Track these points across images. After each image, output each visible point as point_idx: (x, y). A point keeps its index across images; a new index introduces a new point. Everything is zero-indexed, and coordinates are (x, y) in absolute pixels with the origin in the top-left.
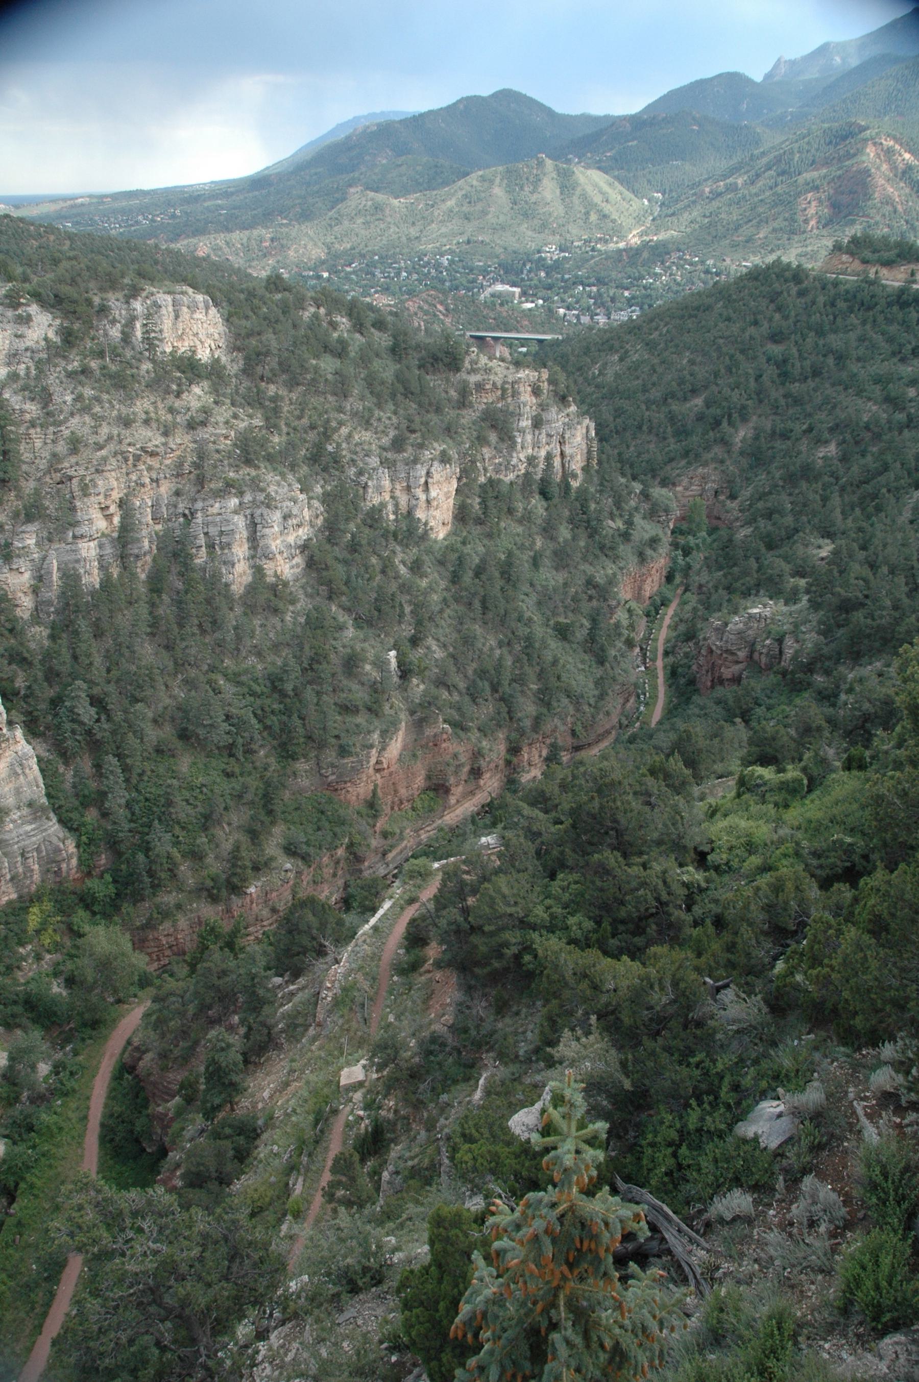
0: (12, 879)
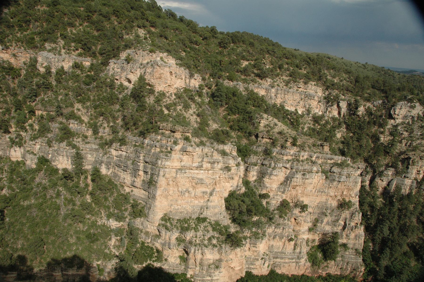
0: (341, 268)
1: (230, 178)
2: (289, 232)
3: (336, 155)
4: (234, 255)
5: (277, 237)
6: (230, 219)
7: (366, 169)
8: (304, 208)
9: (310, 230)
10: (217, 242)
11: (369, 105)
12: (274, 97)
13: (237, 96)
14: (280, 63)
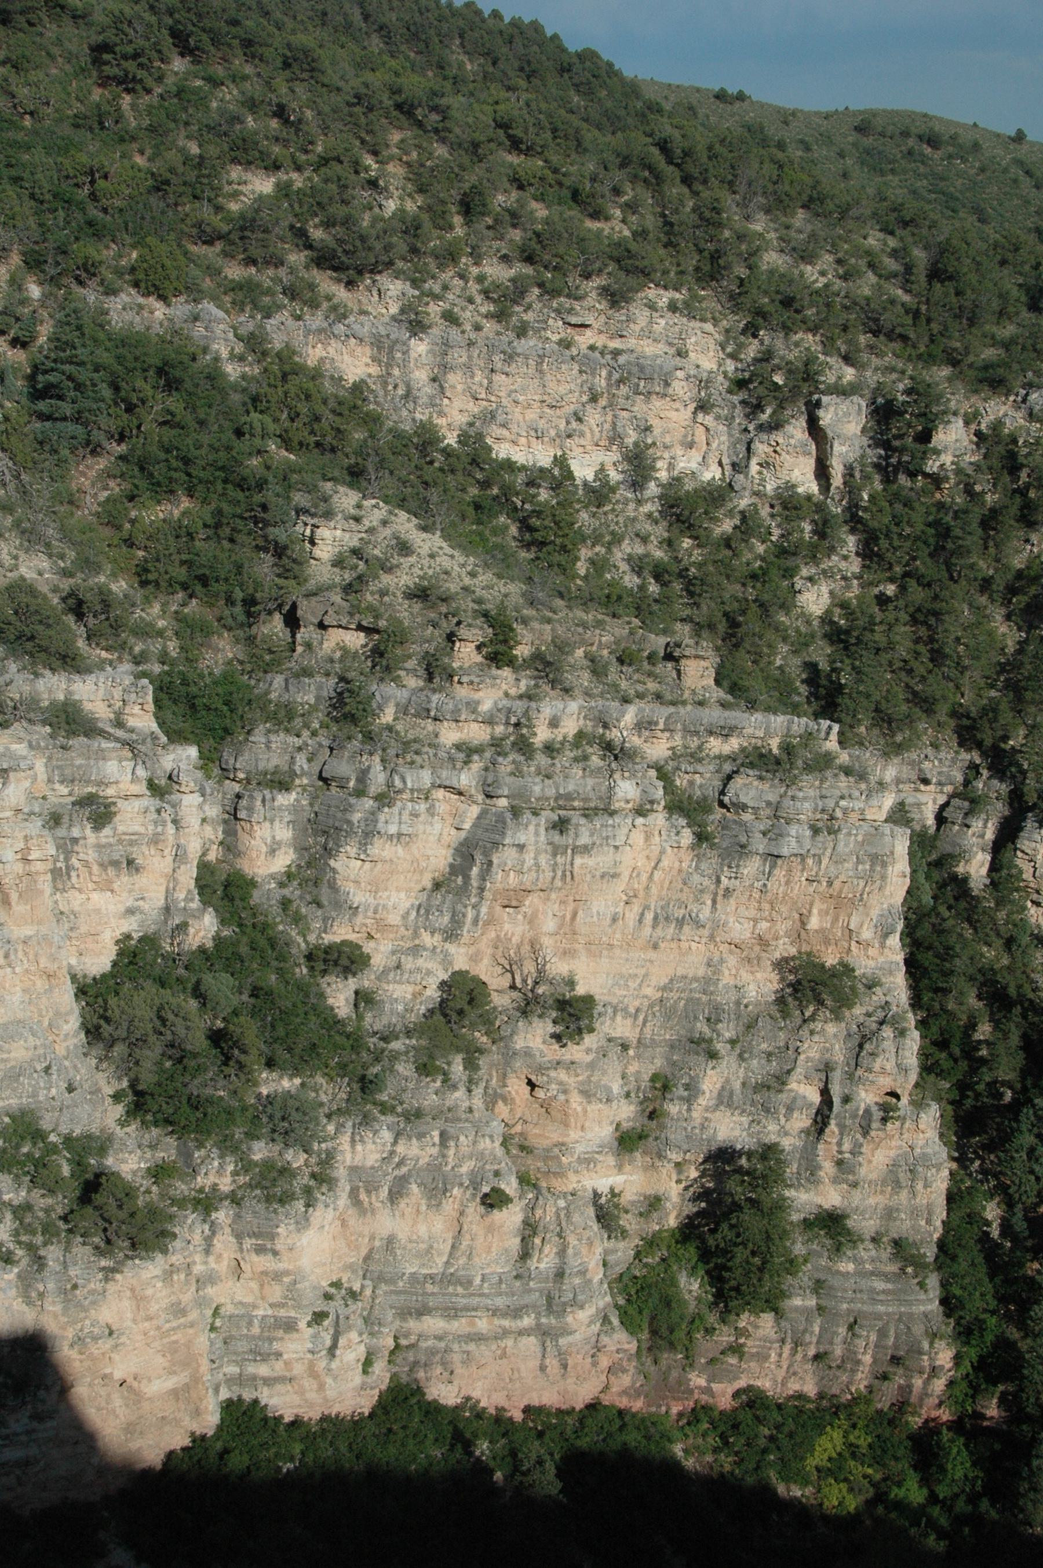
0: (817, 1357)
1: (115, 864)
2: (480, 1156)
3: (752, 706)
4: (127, 1304)
5: (414, 1188)
6: (117, 1097)
7: (967, 783)
8: (573, 1014)
9: (627, 1142)
10: (16, 1233)
11: (1003, 409)
12: (429, 390)
13: (188, 385)
14: (471, 179)
